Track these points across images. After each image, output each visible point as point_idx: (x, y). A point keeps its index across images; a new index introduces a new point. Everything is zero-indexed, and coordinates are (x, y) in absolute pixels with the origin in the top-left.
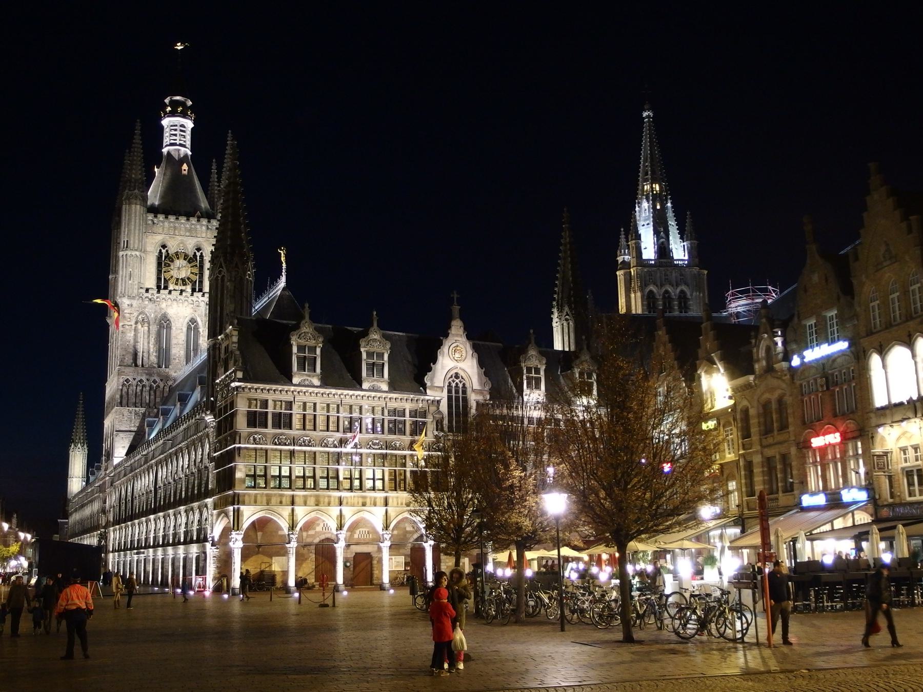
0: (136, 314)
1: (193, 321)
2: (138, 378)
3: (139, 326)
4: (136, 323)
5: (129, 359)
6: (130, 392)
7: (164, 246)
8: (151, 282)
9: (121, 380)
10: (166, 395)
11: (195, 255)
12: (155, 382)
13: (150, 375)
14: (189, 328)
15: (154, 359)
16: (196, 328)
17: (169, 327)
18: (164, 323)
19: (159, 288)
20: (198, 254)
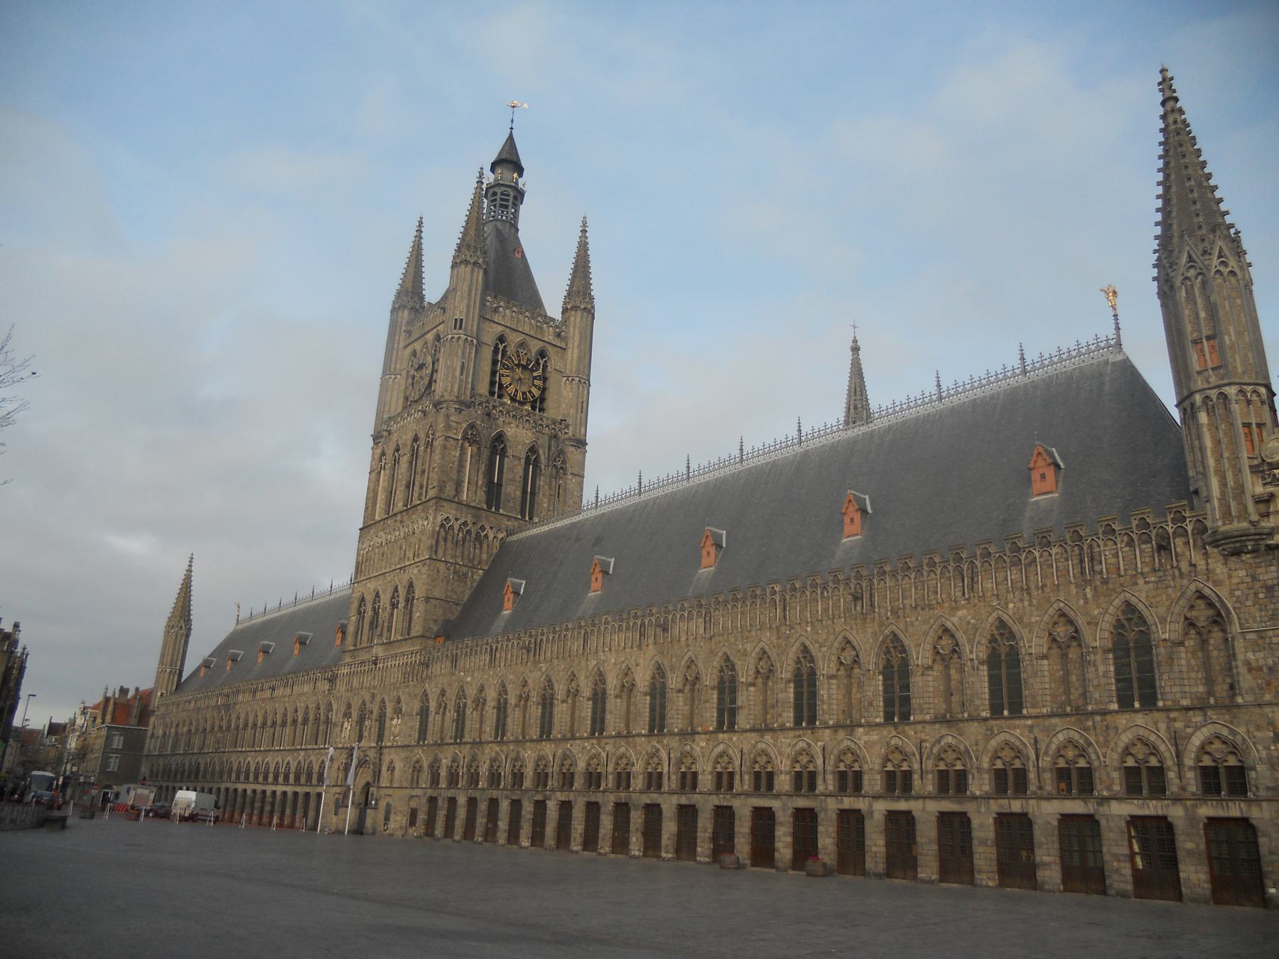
0: (464, 425)
1: (533, 450)
2: (462, 521)
3: (467, 444)
4: (464, 438)
5: (450, 490)
6: (450, 537)
7: (501, 339)
8: (483, 388)
9: (440, 519)
10: (495, 551)
11: (538, 363)
12: (483, 528)
13: (477, 518)
14: (528, 459)
15: (480, 498)
16: (536, 464)
17: (503, 454)
18: (498, 444)
19: (492, 393)
20: (541, 362)
